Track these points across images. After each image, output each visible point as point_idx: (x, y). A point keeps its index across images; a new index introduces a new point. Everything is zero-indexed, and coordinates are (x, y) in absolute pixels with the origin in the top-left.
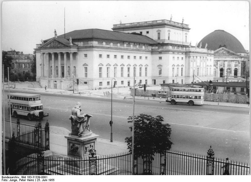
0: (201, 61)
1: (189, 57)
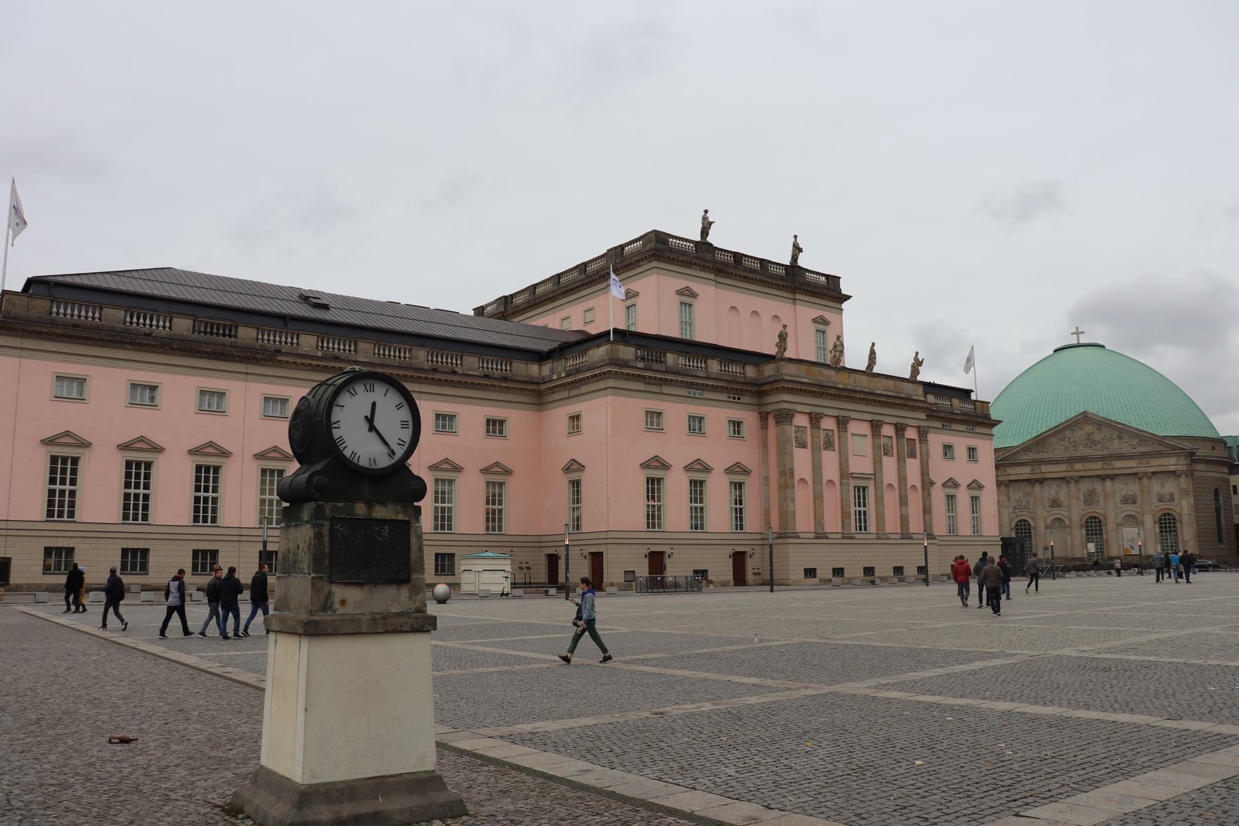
0: (880, 451)
1: (784, 417)
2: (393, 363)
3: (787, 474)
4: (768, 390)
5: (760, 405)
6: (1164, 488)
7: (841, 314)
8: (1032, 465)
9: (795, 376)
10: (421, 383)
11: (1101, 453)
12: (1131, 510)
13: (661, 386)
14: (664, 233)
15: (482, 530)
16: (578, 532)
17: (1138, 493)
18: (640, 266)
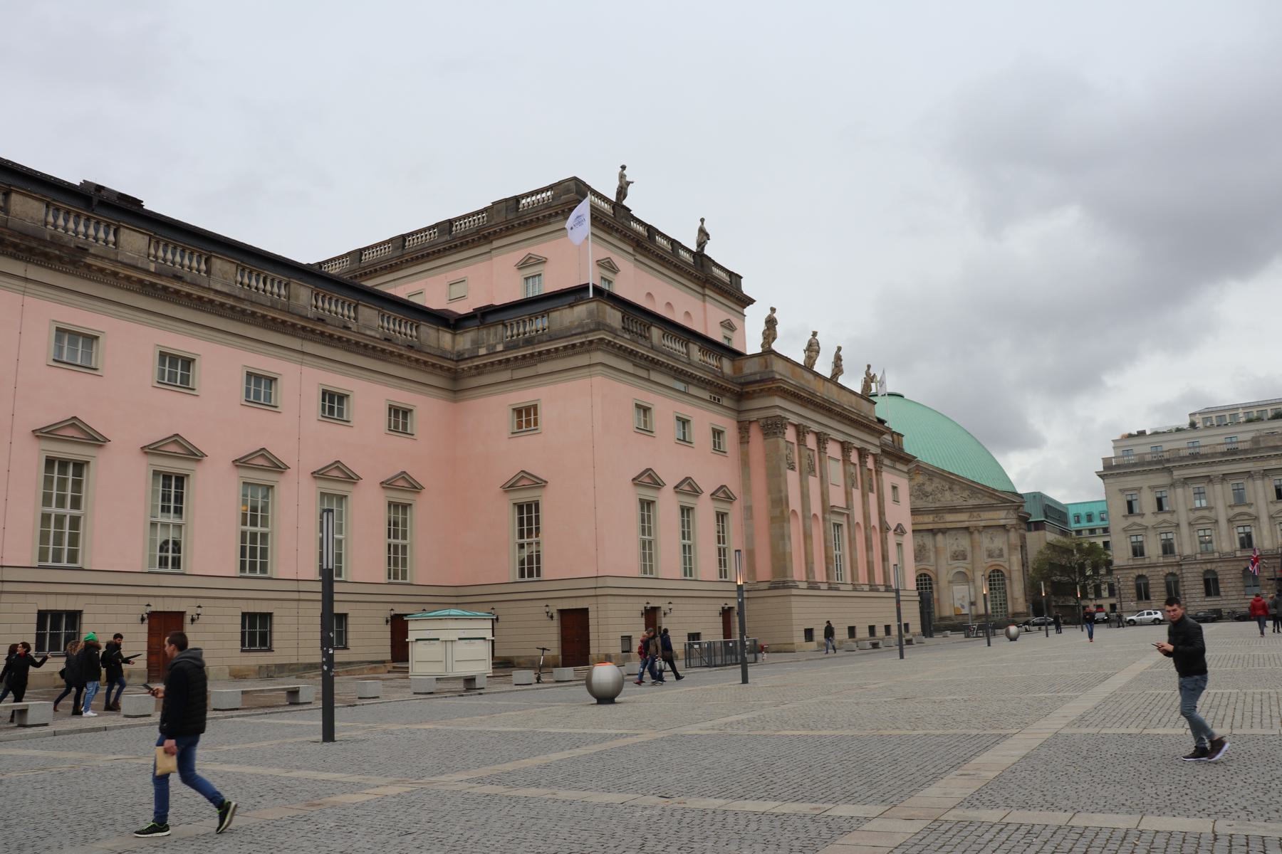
1: (773, 427)
2: (263, 300)
3: (779, 501)
4: (754, 391)
5: (739, 412)
6: (993, 542)
7: (744, 321)
8: (937, 513)
9: (788, 378)
10: (304, 339)
11: (933, 505)
12: (961, 565)
13: (648, 370)
14: (584, 184)
15: (383, 578)
16: (530, 579)
17: (969, 549)
18: (550, 224)
